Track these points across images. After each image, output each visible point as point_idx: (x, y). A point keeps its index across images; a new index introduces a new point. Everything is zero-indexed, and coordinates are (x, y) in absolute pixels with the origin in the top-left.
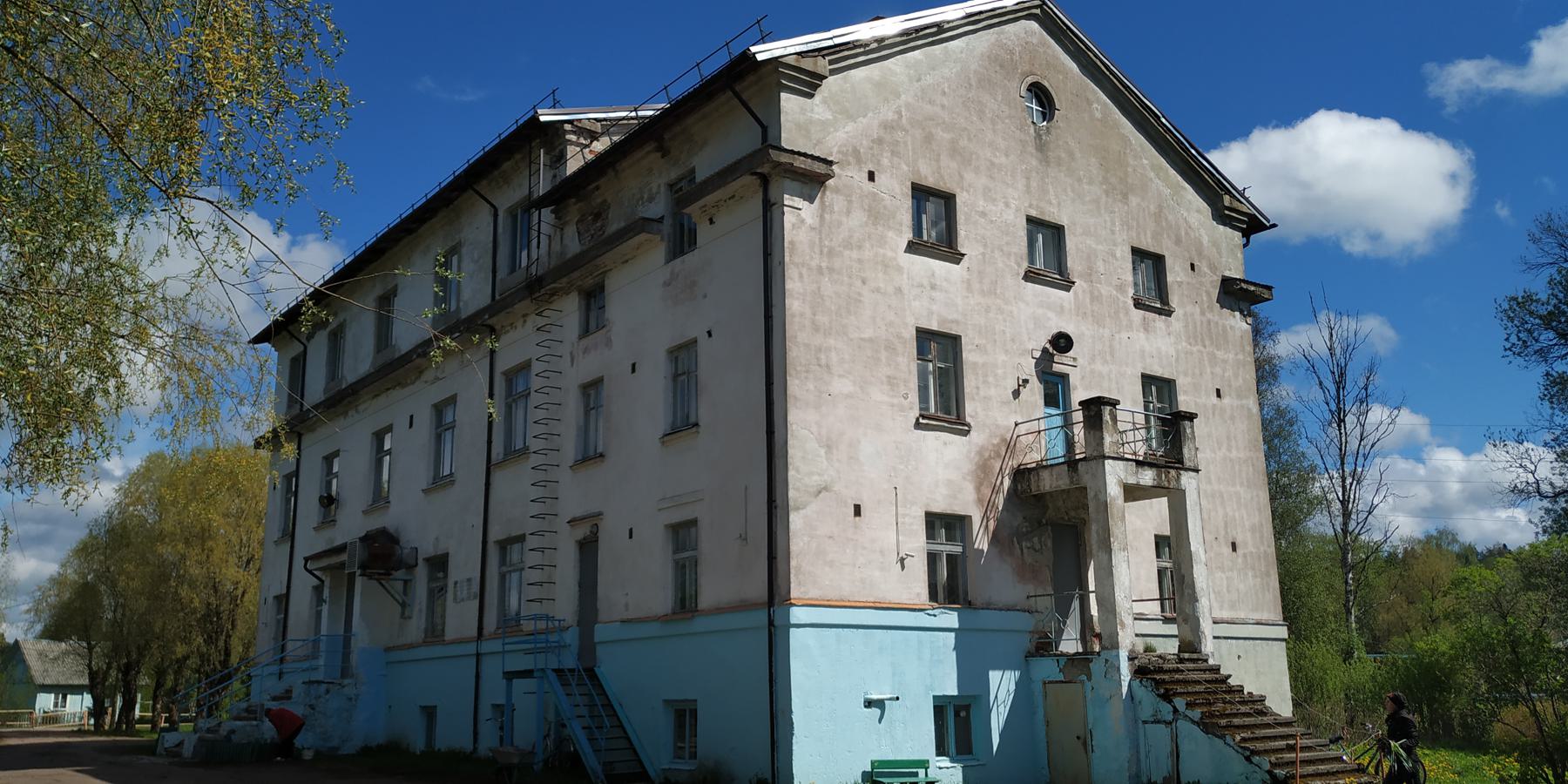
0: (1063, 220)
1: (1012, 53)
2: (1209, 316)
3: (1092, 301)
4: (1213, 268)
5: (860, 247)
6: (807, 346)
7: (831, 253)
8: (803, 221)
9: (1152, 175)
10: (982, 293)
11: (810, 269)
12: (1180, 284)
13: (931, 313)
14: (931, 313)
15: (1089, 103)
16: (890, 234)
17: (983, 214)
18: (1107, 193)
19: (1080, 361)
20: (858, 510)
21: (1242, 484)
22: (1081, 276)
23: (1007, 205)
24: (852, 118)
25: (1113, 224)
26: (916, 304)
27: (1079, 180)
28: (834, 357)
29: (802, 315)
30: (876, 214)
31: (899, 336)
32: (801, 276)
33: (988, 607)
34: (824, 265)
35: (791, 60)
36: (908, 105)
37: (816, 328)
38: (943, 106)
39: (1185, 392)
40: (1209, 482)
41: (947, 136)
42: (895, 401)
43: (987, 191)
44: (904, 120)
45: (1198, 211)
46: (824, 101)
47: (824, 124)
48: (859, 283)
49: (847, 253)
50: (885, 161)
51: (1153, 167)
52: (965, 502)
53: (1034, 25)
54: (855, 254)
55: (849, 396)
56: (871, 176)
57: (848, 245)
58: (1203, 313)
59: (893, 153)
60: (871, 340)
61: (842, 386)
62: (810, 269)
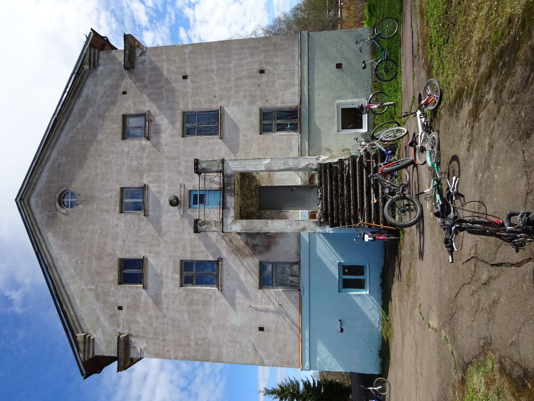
0: (118, 187)
1: (49, 217)
2: (147, 82)
3: (152, 171)
4: (122, 78)
5: (151, 317)
6: (196, 350)
7: (156, 334)
8: (145, 348)
9: (84, 121)
10: (159, 245)
11: (164, 346)
12: (135, 104)
13: (173, 278)
14: (173, 278)
15: (60, 165)
16: (142, 299)
17: (124, 241)
18: (100, 156)
19: (181, 181)
20: (261, 329)
21: (229, 62)
22: (141, 177)
23: (117, 226)
24: (98, 318)
25: (113, 152)
26: (170, 286)
27: (97, 175)
28: (199, 336)
29: (184, 352)
30: (135, 307)
31: (185, 298)
32: (168, 351)
33: (299, 254)
34: (161, 339)
35: (82, 355)
36: (87, 285)
37: (188, 345)
38: (82, 263)
39: (187, 104)
40: (230, 88)
41: (94, 262)
42: (213, 302)
43: (115, 238)
44: (93, 287)
45: (96, 85)
46: (95, 332)
47: (104, 333)
48: (166, 320)
49: (154, 324)
50: (112, 300)
51: (80, 120)
52: (253, 262)
53: (33, 201)
54: (155, 321)
55: (214, 329)
56: (120, 308)
57: (151, 324)
58: (145, 87)
59: (108, 295)
60: (189, 314)
61: (210, 334)
62: (164, 346)
